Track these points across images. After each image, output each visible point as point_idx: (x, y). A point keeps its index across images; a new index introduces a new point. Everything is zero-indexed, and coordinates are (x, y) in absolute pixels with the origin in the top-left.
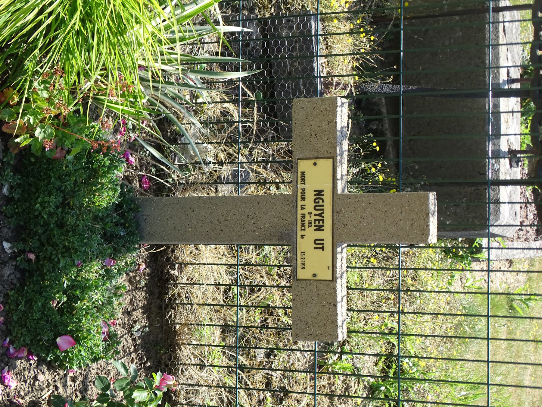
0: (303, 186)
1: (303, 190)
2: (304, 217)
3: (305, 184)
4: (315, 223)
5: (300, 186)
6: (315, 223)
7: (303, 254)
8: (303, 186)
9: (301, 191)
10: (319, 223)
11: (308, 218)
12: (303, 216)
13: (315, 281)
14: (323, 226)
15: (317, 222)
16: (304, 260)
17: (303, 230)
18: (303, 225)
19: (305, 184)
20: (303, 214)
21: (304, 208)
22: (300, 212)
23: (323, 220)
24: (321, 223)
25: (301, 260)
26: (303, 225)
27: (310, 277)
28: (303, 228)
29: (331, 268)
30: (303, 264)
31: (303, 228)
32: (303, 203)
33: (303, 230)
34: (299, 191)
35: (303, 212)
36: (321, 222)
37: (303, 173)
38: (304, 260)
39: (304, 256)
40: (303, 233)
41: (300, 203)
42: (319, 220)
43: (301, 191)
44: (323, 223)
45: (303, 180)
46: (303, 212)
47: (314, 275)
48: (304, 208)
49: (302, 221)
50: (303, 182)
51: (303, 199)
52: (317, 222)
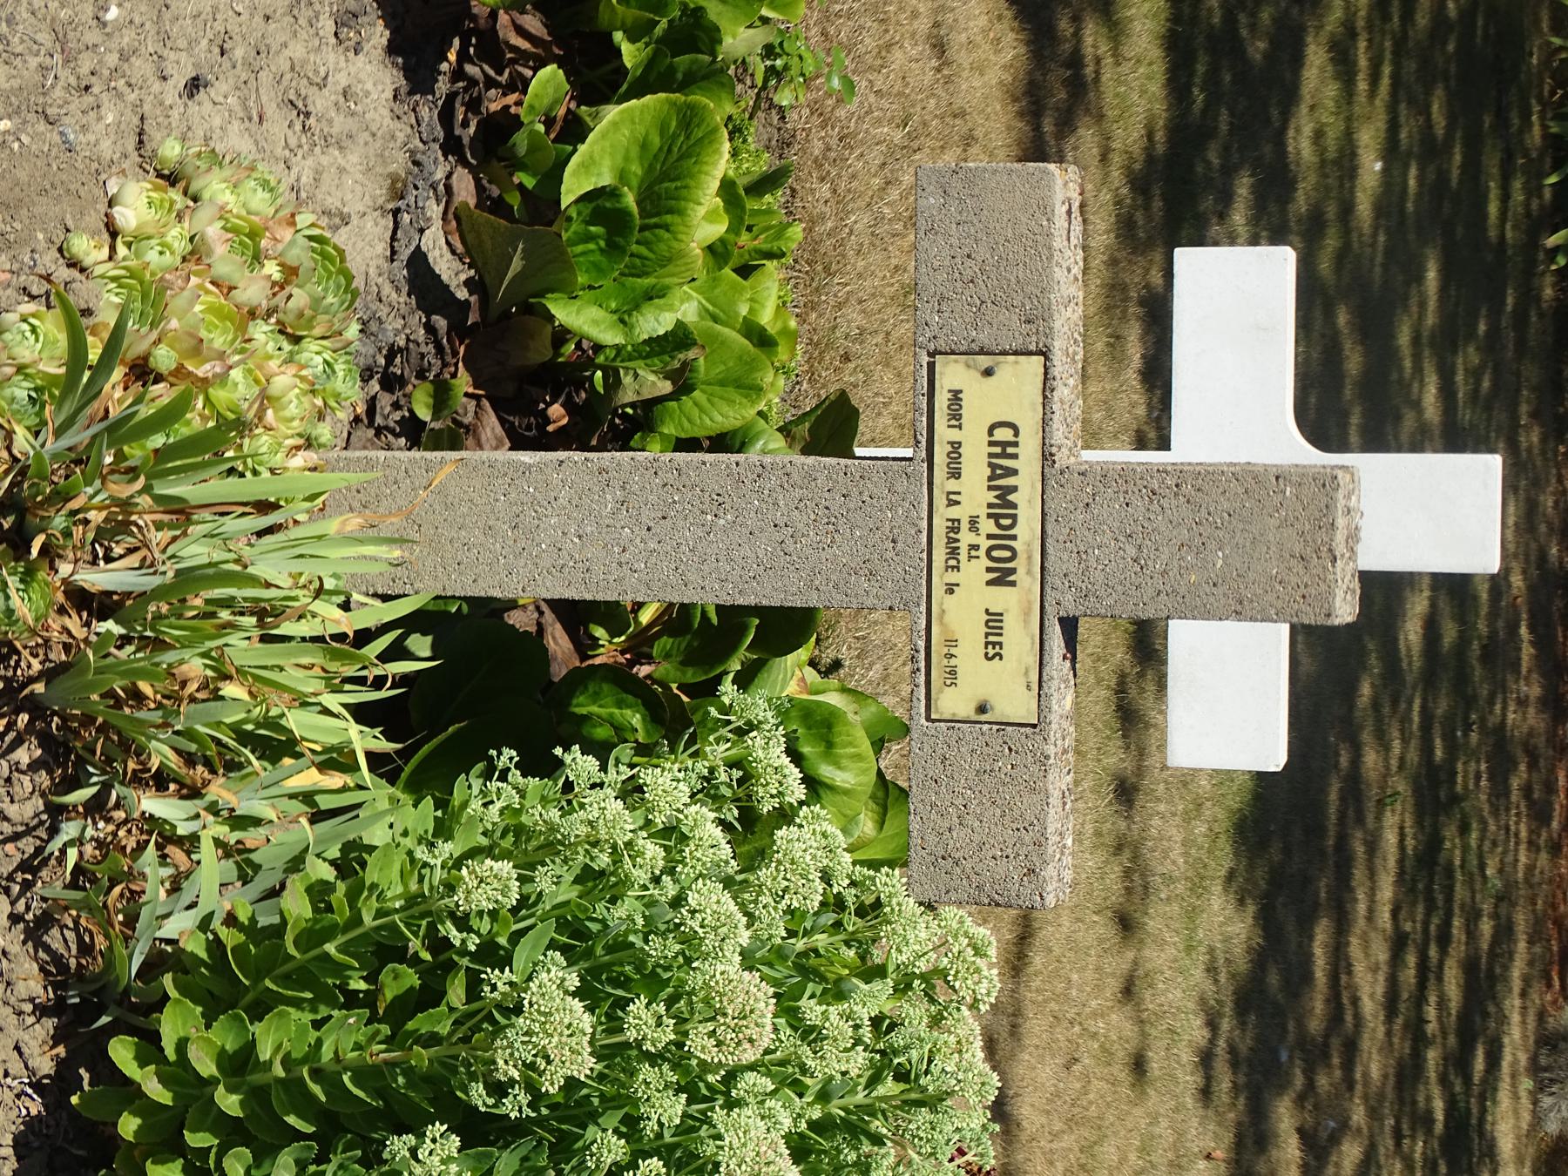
0: (954, 435)
1: (956, 446)
2: (956, 530)
5: (943, 433)
7: (952, 642)
8: (954, 435)
11: (966, 538)
12: (954, 527)
16: (953, 662)
17: (953, 567)
18: (953, 552)
20: (953, 521)
22: (943, 514)
26: (953, 552)
27: (966, 710)
28: (953, 563)
29: (1035, 687)
30: (953, 672)
31: (953, 563)
35: (954, 512)
37: (956, 395)
40: (952, 577)
45: (955, 415)
46: (954, 512)
49: (951, 540)
50: (953, 422)
51: (955, 474)
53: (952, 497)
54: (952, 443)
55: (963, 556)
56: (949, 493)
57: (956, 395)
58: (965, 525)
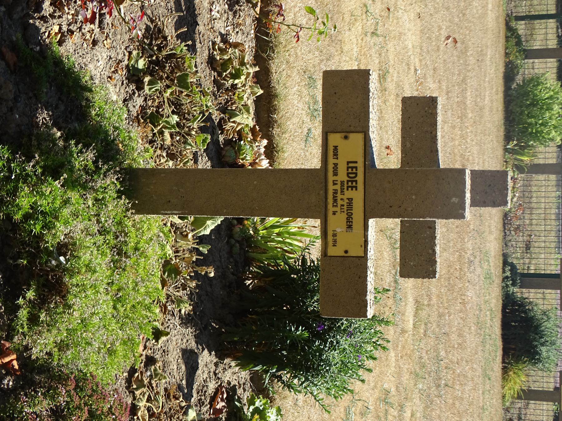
0: (335, 161)
1: (336, 165)
2: (337, 193)
3: (337, 158)
5: (331, 161)
8: (335, 161)
9: (334, 166)
13: (345, 257)
16: (335, 238)
17: (335, 206)
18: (335, 201)
19: (337, 158)
20: (335, 190)
21: (337, 184)
22: (331, 188)
26: (335, 201)
28: (335, 204)
30: (335, 241)
31: (335, 204)
32: (335, 178)
33: (335, 206)
35: (336, 187)
37: (336, 148)
38: (335, 238)
40: (335, 209)
41: (331, 178)
43: (334, 166)
45: (336, 155)
46: (336, 187)
47: (346, 252)
48: (337, 184)
49: (334, 197)
51: (335, 174)
56: (333, 181)
57: (336, 148)
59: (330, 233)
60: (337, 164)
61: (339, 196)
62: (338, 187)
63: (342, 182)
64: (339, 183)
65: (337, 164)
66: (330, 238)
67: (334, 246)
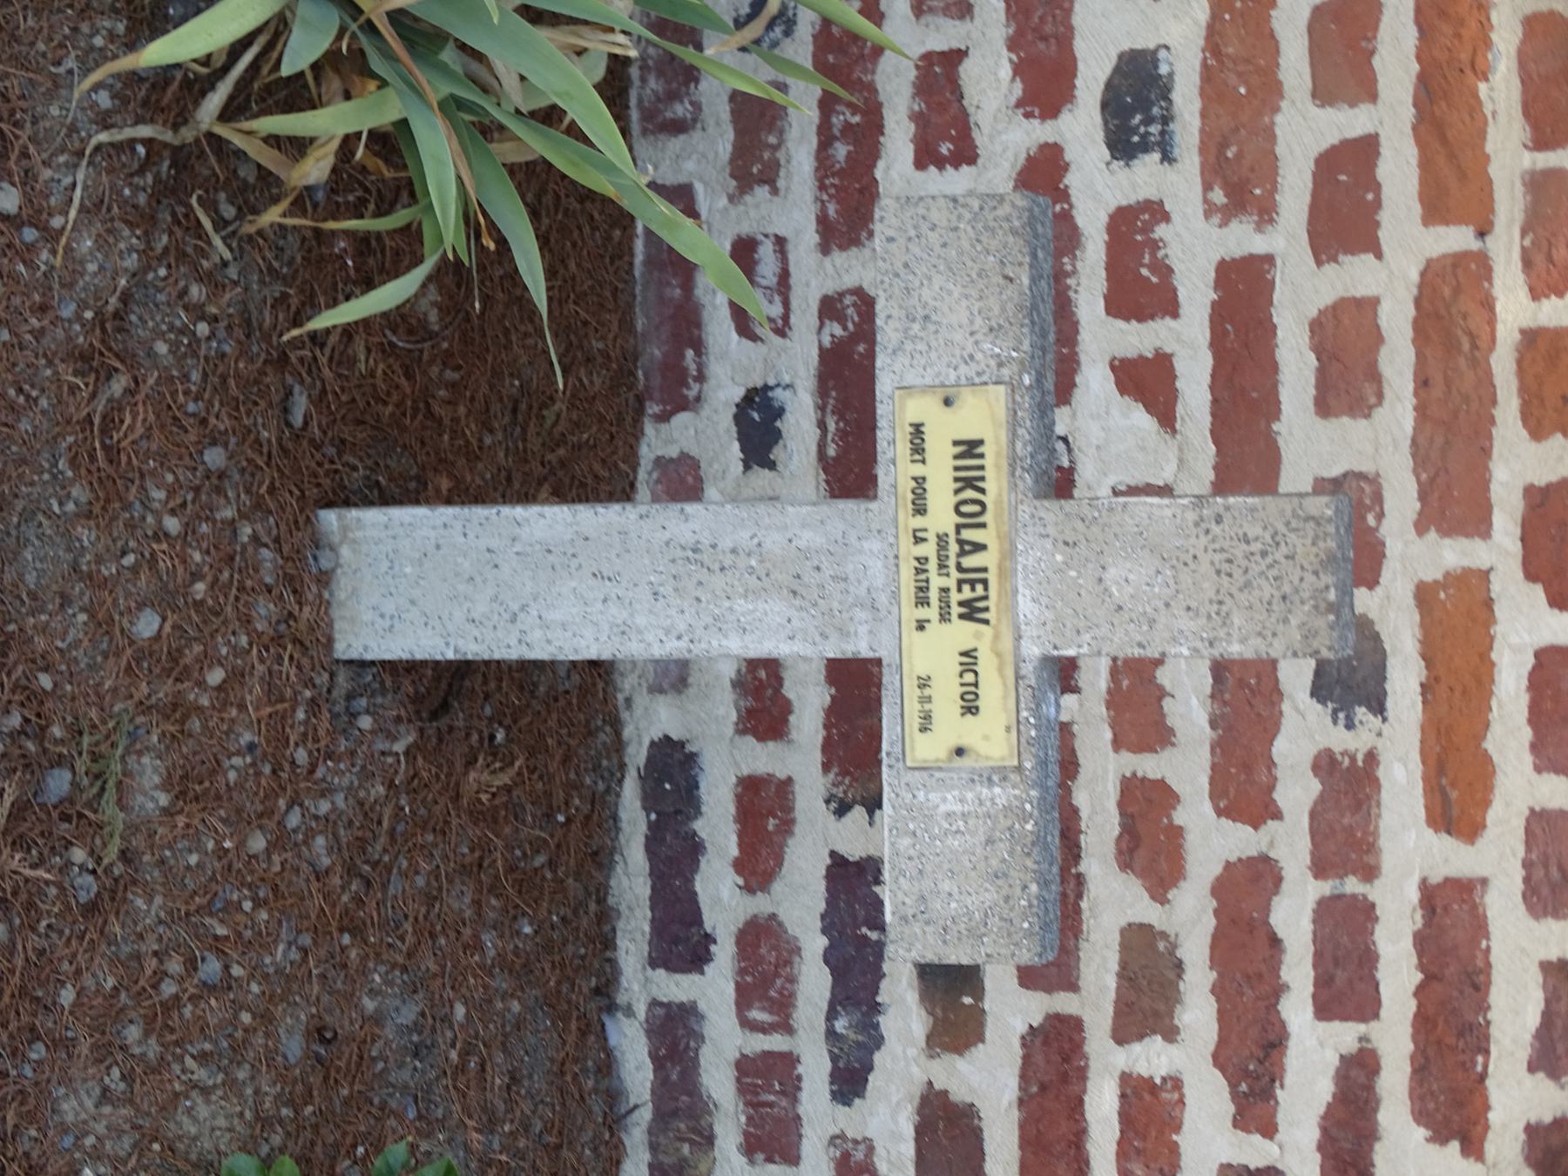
0: (918, 470)
1: (920, 481)
3: (923, 462)
4: (960, 590)
6: (960, 590)
7: (924, 683)
8: (918, 470)
10: (973, 589)
14: (986, 598)
15: (966, 588)
16: (927, 707)
19: (923, 462)
20: (917, 559)
23: (985, 582)
24: (979, 588)
25: (918, 706)
30: (927, 717)
32: (918, 522)
34: (906, 486)
35: (921, 550)
36: (979, 588)
37: (918, 429)
38: (927, 707)
39: (927, 692)
42: (972, 583)
43: (913, 484)
44: (986, 589)
45: (918, 450)
46: (921, 550)
50: (917, 457)
51: (920, 510)
52: (966, 588)
53: (919, 534)
54: (915, 479)
55: (934, 595)
58: (932, 565)
59: (911, 692)
60: (924, 479)
61: (936, 582)
62: (929, 549)
63: (942, 540)
64: (931, 536)
65: (924, 479)
66: (913, 709)
67: (924, 729)
